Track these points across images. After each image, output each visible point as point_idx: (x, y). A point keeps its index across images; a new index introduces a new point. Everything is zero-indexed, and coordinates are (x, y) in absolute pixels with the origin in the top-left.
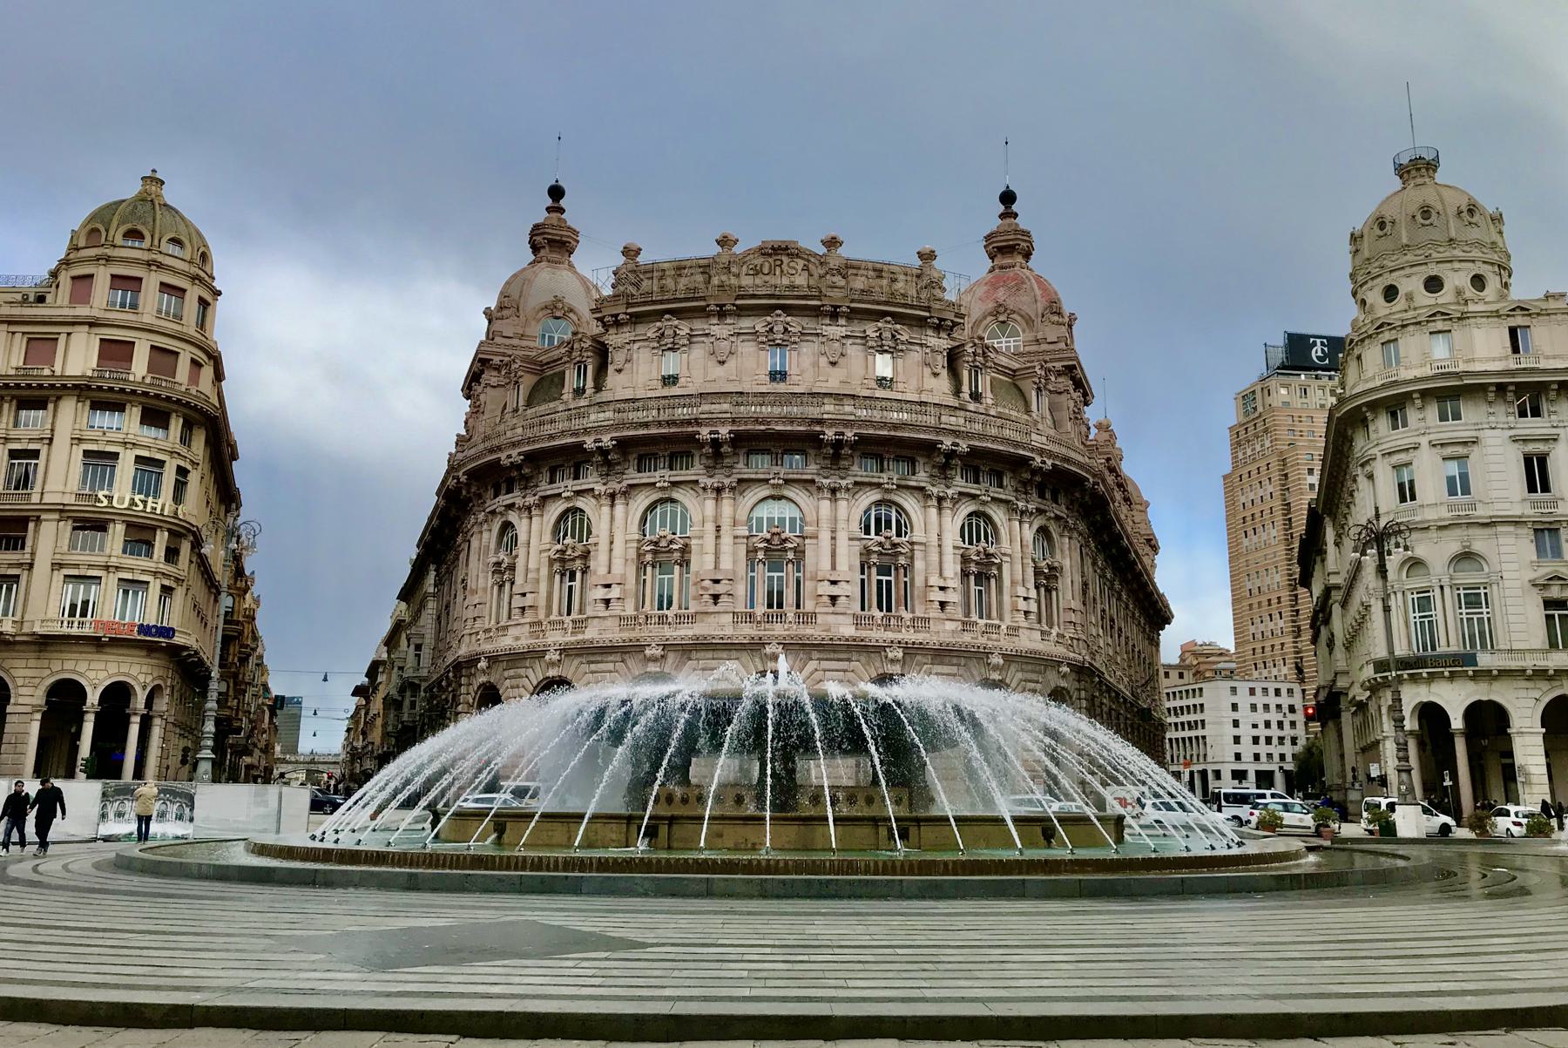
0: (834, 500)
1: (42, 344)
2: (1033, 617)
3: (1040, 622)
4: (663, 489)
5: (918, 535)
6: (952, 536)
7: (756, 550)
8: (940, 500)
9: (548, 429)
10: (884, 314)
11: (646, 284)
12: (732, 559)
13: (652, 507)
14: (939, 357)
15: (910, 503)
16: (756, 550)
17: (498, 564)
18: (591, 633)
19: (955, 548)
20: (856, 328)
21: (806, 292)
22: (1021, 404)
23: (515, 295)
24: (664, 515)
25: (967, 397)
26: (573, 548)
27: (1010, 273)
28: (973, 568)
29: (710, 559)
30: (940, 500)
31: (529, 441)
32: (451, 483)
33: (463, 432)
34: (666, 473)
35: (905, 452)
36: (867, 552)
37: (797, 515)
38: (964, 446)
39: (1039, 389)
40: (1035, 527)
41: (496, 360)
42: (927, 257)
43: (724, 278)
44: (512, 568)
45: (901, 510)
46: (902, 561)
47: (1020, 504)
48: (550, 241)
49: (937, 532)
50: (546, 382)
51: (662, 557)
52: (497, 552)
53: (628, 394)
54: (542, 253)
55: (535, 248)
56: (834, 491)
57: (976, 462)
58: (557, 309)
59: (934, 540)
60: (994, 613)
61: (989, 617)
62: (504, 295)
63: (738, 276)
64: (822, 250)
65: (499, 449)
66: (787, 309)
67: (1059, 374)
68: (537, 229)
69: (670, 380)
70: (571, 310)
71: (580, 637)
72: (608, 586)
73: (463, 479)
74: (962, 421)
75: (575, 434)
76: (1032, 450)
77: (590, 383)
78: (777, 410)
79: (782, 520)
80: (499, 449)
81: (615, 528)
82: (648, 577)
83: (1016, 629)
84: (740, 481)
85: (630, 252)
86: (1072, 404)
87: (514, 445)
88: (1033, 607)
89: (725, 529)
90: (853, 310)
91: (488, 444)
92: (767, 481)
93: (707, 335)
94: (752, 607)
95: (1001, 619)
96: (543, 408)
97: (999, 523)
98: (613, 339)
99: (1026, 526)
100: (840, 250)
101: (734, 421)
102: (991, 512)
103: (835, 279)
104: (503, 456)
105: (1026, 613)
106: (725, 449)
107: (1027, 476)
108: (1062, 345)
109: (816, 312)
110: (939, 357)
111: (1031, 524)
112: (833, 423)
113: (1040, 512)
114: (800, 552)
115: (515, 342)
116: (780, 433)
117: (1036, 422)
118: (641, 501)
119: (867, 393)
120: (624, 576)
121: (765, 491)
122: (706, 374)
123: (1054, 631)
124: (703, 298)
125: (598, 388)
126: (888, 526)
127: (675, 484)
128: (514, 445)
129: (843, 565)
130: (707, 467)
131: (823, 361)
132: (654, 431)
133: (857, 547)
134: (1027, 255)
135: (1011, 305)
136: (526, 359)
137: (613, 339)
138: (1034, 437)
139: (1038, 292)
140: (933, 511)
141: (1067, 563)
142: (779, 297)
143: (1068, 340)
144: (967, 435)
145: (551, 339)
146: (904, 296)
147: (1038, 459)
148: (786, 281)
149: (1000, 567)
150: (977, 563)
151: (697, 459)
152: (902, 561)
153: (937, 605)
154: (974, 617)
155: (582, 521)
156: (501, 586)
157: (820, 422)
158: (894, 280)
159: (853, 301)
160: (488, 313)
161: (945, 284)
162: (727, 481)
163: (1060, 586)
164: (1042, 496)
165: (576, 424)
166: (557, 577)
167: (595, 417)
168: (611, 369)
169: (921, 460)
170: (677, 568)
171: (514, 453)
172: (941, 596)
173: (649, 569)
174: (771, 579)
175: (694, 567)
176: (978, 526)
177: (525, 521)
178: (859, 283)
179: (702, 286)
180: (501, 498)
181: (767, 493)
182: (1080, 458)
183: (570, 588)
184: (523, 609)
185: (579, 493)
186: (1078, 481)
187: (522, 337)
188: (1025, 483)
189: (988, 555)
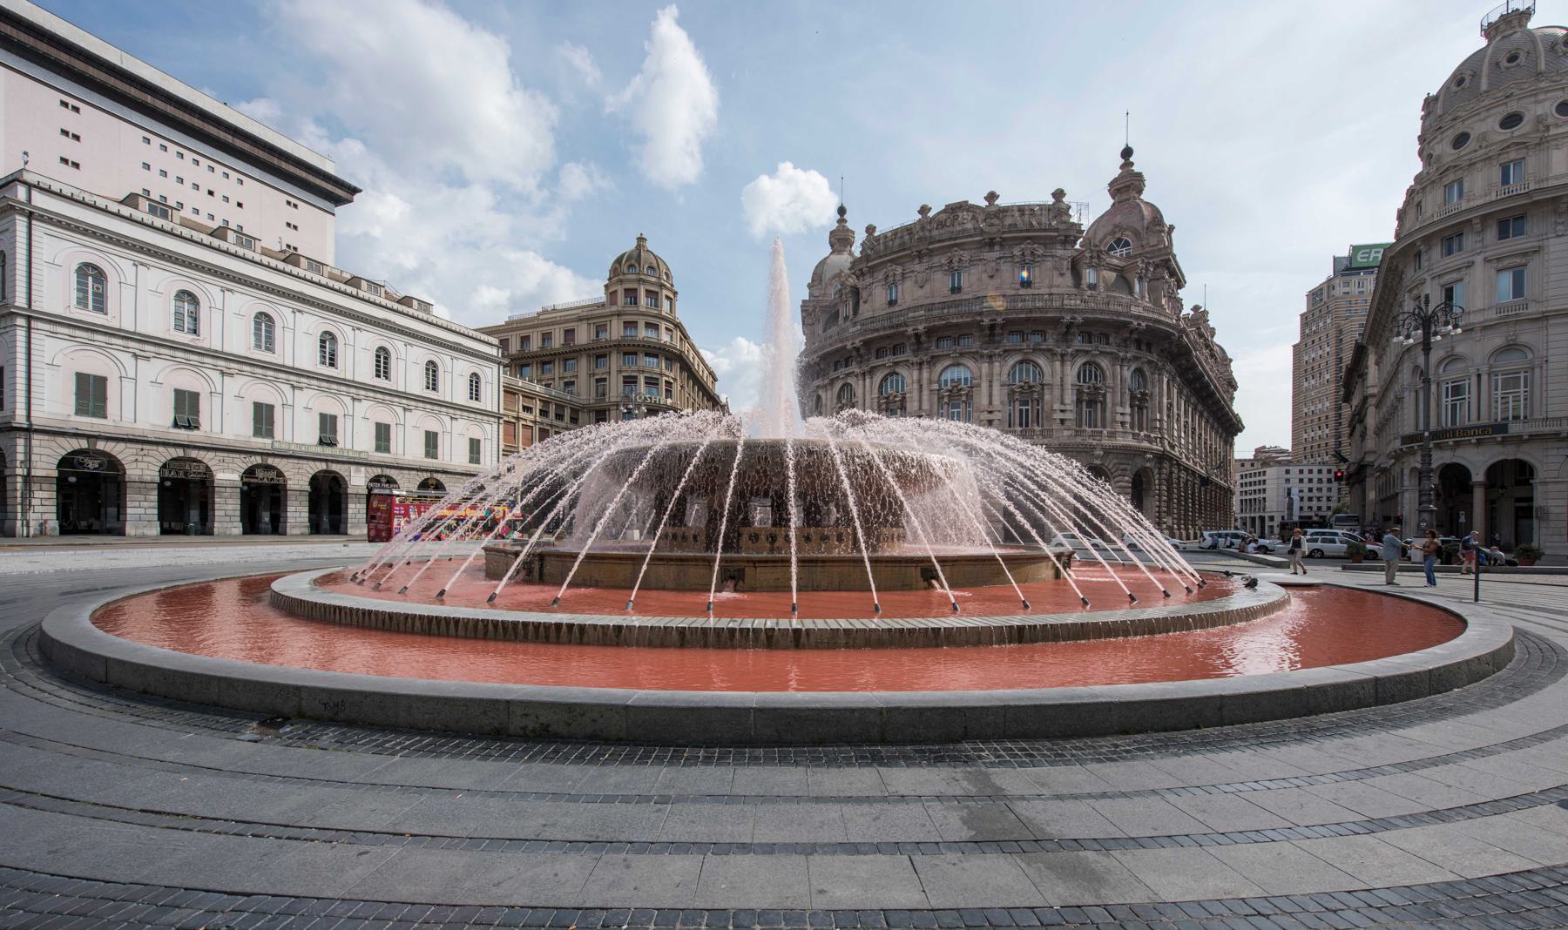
0: (991, 362)
1: (600, 329)
5: (1047, 379)
8: (1062, 356)
13: (885, 379)
15: (1042, 361)
29: (916, 404)
30: (1062, 356)
36: (1011, 393)
38: (1079, 319)
45: (1036, 365)
46: (1036, 396)
49: (1061, 377)
51: (892, 406)
56: (990, 357)
88: (1128, 419)
102: (1098, 360)
106: (923, 338)
113: (1136, 358)
114: (969, 396)
116: (956, 325)
118: (879, 376)
125: (856, 312)
127: (896, 364)
129: (996, 402)
133: (1006, 390)
140: (1058, 364)
144: (1082, 311)
149: (1104, 396)
152: (1036, 396)
157: (980, 314)
172: (1061, 416)
176: (1091, 370)
185: (848, 375)
186: (1167, 336)
189: (1096, 388)
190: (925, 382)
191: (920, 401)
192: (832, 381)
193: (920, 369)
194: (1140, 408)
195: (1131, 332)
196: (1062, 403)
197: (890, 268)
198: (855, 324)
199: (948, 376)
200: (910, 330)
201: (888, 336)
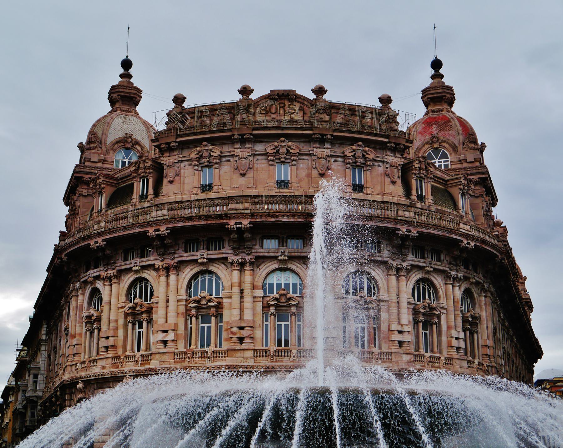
2: (462, 351)
3: (466, 354)
4: (202, 264)
5: (383, 295)
6: (406, 297)
7: (269, 306)
8: (398, 270)
9: (123, 223)
10: (356, 140)
11: (189, 122)
12: (252, 311)
13: (195, 277)
14: (396, 171)
16: (269, 306)
17: (89, 317)
18: (154, 364)
19: (409, 303)
20: (338, 150)
21: (302, 125)
22: (451, 203)
23: (99, 134)
24: (203, 282)
25: (414, 197)
26: (141, 306)
27: (440, 115)
28: (421, 318)
29: (236, 312)
30: (398, 270)
31: (110, 231)
32: (57, 261)
33: (64, 230)
34: (205, 253)
37: (298, 281)
38: (414, 232)
39: (463, 195)
40: (463, 289)
41: (87, 177)
42: (386, 100)
43: (244, 116)
44: (99, 319)
45: (371, 278)
47: (453, 273)
50: (121, 194)
51: (203, 312)
52: (88, 308)
53: (178, 198)
54: (117, 105)
55: (112, 101)
58: (127, 143)
59: (394, 297)
60: (436, 349)
61: (432, 351)
62: (92, 133)
63: (254, 114)
64: (312, 96)
65: (89, 237)
66: (290, 137)
67: (476, 183)
68: (113, 89)
69: (207, 188)
70: (137, 143)
71: (147, 367)
72: (166, 332)
73: (65, 259)
74: (412, 214)
75: (142, 225)
76: (462, 235)
77: (151, 191)
78: (282, 207)
79: (287, 285)
80: (89, 237)
81: (170, 291)
82: (193, 326)
83: (451, 359)
84: (257, 258)
85: (179, 100)
86: (485, 205)
87: (99, 234)
88: (462, 345)
89: (247, 292)
92: (275, 258)
93: (232, 156)
94: (267, 345)
95: (440, 353)
96: (119, 209)
97: (438, 286)
98: (167, 160)
99: (457, 288)
100: (324, 97)
101: (252, 215)
102: (433, 279)
103: (322, 116)
104: (92, 242)
105: (458, 349)
106: (247, 235)
107: (457, 253)
108: (478, 164)
109: (309, 139)
110: (396, 171)
111: (460, 287)
113: (466, 278)
115: (99, 165)
117: (462, 217)
118: (188, 273)
120: (176, 325)
121: (274, 265)
122: (232, 183)
123: (476, 361)
124: (230, 130)
125: (157, 193)
126: (362, 288)
128: (99, 234)
130: (233, 248)
131: (315, 173)
132: (196, 223)
135: (441, 136)
136: (106, 176)
137: (167, 160)
138: (462, 226)
139: (460, 128)
140: (394, 278)
141: (484, 314)
143: (480, 160)
145: (124, 163)
146: (371, 127)
147: (465, 242)
148: (287, 118)
149: (439, 317)
150: (424, 314)
151: (226, 245)
153: (396, 344)
154: (422, 352)
155: (146, 287)
156: (92, 333)
159: (335, 131)
160: (80, 146)
161: (398, 119)
162: (248, 258)
163: (480, 330)
164: (466, 267)
165: (142, 219)
166: (130, 326)
167: (156, 214)
168: (165, 181)
170: (213, 319)
171: (99, 240)
172: (399, 337)
173: (194, 320)
174: (279, 326)
175: (225, 318)
177: (107, 288)
178: (339, 119)
179: (229, 121)
180: (91, 272)
181: (275, 266)
182: (492, 241)
183: (139, 333)
184: (107, 348)
185: (144, 268)
187: (104, 161)
188: (455, 258)
189: (432, 309)
190: (247, 287)
191: (241, 309)
192: (121, 273)
193: (241, 271)
194: (472, 334)
196: (399, 323)
198: (159, 206)
199: (274, 279)
200: (232, 223)
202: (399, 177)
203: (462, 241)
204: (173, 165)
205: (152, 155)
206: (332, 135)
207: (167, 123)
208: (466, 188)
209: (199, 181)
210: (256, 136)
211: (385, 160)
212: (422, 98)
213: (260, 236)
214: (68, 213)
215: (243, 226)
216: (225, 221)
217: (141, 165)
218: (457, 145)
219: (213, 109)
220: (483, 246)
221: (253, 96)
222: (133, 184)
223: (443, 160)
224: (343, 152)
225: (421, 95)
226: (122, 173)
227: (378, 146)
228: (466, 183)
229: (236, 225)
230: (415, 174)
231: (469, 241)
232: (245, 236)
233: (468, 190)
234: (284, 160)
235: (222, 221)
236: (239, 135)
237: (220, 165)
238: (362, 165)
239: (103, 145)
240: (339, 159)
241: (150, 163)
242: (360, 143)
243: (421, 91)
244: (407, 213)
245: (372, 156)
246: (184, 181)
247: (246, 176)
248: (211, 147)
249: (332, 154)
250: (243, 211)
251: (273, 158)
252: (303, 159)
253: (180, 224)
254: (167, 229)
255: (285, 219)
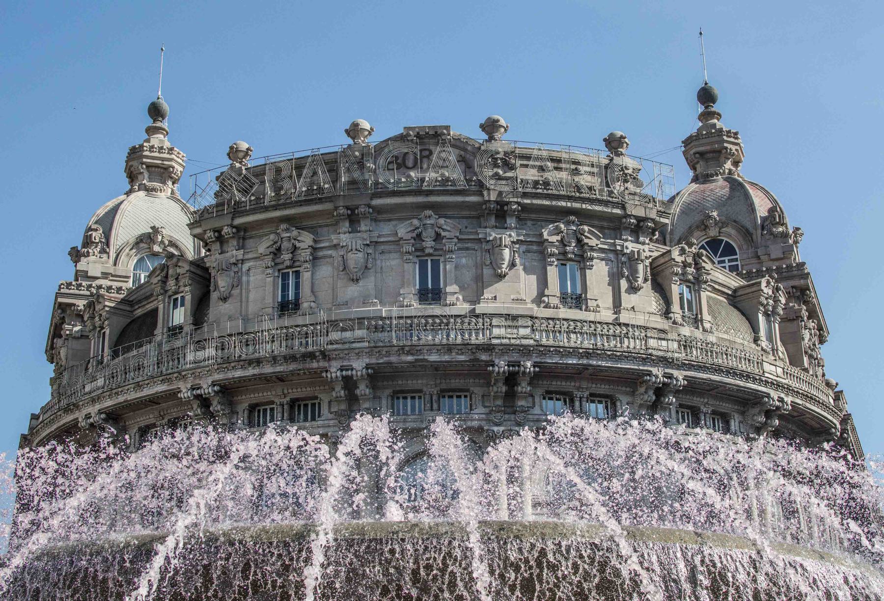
35: (603, 389)
39: (766, 314)
43: (356, 175)
48: (149, 166)
55: (132, 176)
57: (696, 401)
65: (77, 406)
68: (135, 153)
70: (172, 244)
87: (93, 401)
90: (525, 208)
91: (64, 403)
93: (335, 247)
106: (363, 389)
112: (506, 349)
116: (436, 367)
119: (548, 313)
130: (338, 415)
132: (268, 369)
134: (736, 163)
142: (429, 193)
146: (590, 188)
157: (488, 348)
158: (576, 172)
159: (525, 195)
168: (214, 296)
169: (624, 399)
171: (93, 409)
178: (531, 175)
195: (769, 414)
197: (287, 233)
198: (200, 345)
201: (280, 378)
202: (646, 280)
203: (768, 396)
204: (228, 269)
205: (190, 255)
206: (518, 203)
207: (216, 195)
208: (771, 302)
209: (274, 296)
210: (379, 210)
211: (619, 248)
212: (685, 153)
213: (388, 392)
214: (53, 375)
215: (354, 372)
216: (323, 364)
217: (171, 272)
218: (751, 230)
219: (299, 165)
220: (808, 405)
221: (373, 140)
222: (155, 311)
223: (726, 259)
224: (541, 235)
225: (683, 149)
226: (141, 293)
227: (605, 224)
228: (770, 293)
229: (342, 371)
230: (676, 274)
231: (782, 395)
232: (358, 392)
233: (774, 307)
234: (431, 251)
235: (315, 365)
236: (347, 208)
237: (314, 266)
238: (577, 259)
239: (111, 247)
240: (535, 248)
241: (185, 268)
242: (572, 218)
243: (683, 142)
244: (664, 343)
245: (593, 242)
246: (247, 298)
247: (361, 283)
248: (295, 233)
249: (522, 238)
250: (354, 345)
251: (411, 249)
252: (467, 249)
253: (238, 373)
254: (214, 384)
255: (433, 358)
